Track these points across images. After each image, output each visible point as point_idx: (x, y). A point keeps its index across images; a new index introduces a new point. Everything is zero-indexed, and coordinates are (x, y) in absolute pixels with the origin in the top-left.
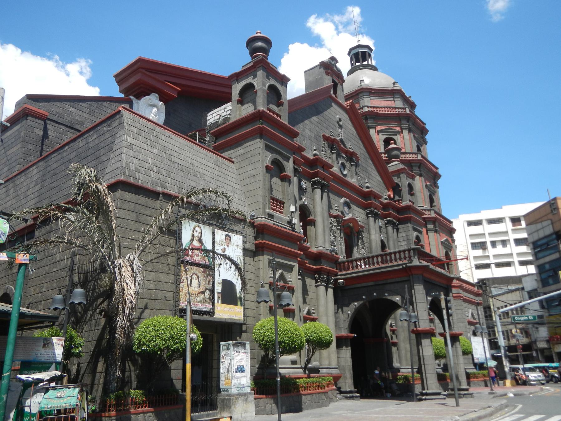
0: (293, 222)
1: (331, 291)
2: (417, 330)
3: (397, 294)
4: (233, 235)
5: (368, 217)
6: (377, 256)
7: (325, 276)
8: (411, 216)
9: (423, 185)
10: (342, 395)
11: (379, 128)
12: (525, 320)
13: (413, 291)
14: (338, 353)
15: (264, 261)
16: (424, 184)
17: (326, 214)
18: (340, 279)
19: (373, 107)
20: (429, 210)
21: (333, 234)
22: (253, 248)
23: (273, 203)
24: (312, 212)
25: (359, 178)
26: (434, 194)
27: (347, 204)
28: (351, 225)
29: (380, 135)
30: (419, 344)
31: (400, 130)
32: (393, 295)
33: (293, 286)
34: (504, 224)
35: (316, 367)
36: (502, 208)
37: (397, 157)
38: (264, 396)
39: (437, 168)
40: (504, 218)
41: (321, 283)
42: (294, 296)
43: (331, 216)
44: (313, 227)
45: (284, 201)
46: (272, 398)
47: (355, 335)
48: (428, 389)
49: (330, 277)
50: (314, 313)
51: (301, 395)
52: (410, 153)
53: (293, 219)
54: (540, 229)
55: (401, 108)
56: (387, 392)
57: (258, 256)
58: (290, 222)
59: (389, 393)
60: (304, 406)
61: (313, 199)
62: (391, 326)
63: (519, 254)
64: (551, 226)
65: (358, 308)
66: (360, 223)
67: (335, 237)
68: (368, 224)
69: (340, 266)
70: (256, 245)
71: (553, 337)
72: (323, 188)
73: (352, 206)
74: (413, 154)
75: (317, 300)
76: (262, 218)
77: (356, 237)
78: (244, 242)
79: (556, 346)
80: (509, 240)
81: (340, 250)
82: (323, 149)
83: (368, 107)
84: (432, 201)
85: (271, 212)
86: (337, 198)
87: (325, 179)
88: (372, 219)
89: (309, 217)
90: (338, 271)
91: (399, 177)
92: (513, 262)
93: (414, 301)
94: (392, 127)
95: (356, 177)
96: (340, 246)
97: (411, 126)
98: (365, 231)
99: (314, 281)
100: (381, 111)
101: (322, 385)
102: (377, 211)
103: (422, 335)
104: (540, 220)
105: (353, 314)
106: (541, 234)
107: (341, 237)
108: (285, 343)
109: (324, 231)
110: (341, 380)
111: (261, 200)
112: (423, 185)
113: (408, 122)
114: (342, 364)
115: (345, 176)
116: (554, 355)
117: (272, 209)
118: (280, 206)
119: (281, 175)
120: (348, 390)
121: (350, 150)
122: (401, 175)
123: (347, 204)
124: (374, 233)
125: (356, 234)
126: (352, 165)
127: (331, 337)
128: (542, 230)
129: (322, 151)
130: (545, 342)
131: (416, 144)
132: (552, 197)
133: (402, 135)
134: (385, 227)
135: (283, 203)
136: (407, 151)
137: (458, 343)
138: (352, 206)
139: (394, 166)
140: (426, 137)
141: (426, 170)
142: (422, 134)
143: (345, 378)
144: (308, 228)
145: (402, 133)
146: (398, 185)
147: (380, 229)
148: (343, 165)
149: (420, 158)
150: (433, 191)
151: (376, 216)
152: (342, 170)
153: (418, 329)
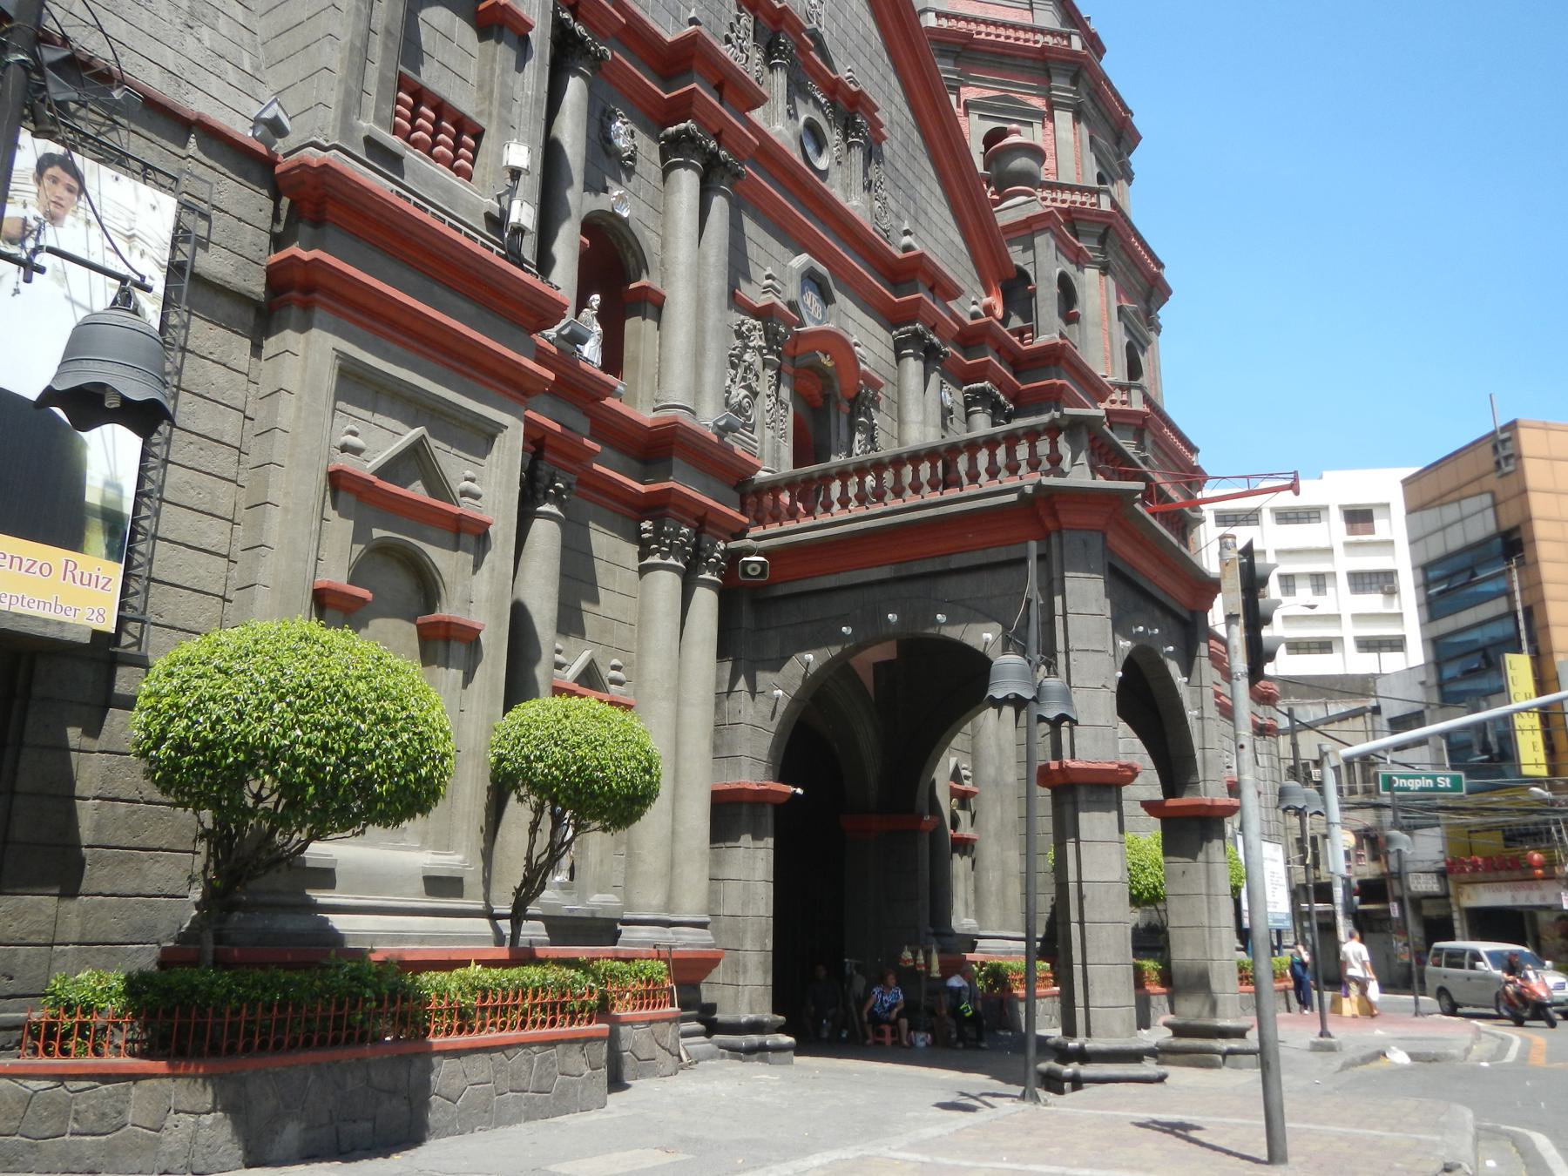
0: (513, 219)
1: (706, 601)
2: (1063, 770)
3: (988, 617)
4: (106, 172)
5: (899, 358)
6: (915, 458)
7: (685, 530)
8: (1063, 386)
9: (1108, 303)
10: (717, 1037)
11: (970, 93)
12: (1422, 789)
13: (1058, 600)
14: (716, 862)
15: (306, 358)
16: (1114, 305)
17: (716, 284)
18: (750, 552)
19: (957, 17)
20: (1122, 387)
21: (744, 379)
22: (256, 285)
23: (416, 114)
24: (653, 260)
25: (877, 204)
26: (1144, 349)
27: (811, 279)
28: (826, 361)
29: (974, 117)
30: (1065, 829)
31: (1045, 109)
32: (969, 621)
33: (485, 517)
34: (1324, 524)
35: (599, 915)
36: (1321, 478)
37: (1029, 179)
38: (161, 1066)
39: (1160, 265)
40: (1326, 508)
41: (665, 556)
42: (485, 567)
43: (735, 301)
44: (650, 324)
45: (482, 122)
46: (205, 1077)
47: (799, 791)
48: (1088, 1034)
49: (705, 537)
50: (619, 683)
51: (428, 1053)
52: (1072, 189)
53: (516, 204)
54: (1450, 525)
55: (1053, 33)
56: (913, 1027)
57: (280, 329)
58: (496, 222)
59: (927, 1030)
60: (436, 1115)
61: (662, 212)
62: (956, 776)
63: (1358, 618)
64: (1490, 513)
65: (816, 675)
66: (863, 366)
67: (756, 394)
68: (899, 384)
69: (760, 501)
70: (272, 273)
71: (1462, 862)
72: (711, 177)
73: (838, 295)
74: (1082, 190)
75: (640, 626)
76: (325, 149)
77: (844, 419)
78: (181, 235)
79: (1468, 889)
80: (1334, 574)
81: (767, 447)
82: (733, 36)
83: (939, 15)
84: (1134, 370)
85: (395, 142)
86: (775, 246)
87: (723, 136)
88: (913, 367)
89: (638, 278)
90: (746, 520)
91: (1029, 246)
92: (1341, 639)
93: (1060, 646)
94: (1017, 96)
95: (865, 195)
96: (769, 433)
97: (1084, 99)
98: (883, 404)
99: (633, 550)
100: (983, 33)
101: (576, 1004)
102: (936, 340)
103: (1082, 794)
104: (1456, 495)
105: (795, 700)
106: (1455, 540)
107: (782, 403)
108: (295, 761)
109: (698, 353)
110: (718, 974)
111: (335, 64)
112: (1108, 303)
113: (1074, 82)
114: (730, 906)
115: (824, 174)
116: (1456, 916)
117: (396, 130)
118: (458, 144)
119: (482, 6)
120: (745, 1017)
121: (852, 86)
122: (1037, 240)
123: (811, 279)
124: (920, 418)
125: (845, 406)
126: (850, 146)
127: (647, 771)
128: (1458, 527)
129: (728, 40)
130: (1435, 876)
131: (1096, 170)
132: (1502, 422)
133: (1049, 125)
134: (963, 416)
135: (478, 135)
136: (1062, 180)
137: (1217, 843)
138: (838, 295)
139: (1010, 212)
140: (1132, 158)
141: (1124, 257)
142: (1118, 144)
143: (738, 967)
144: (631, 325)
145: (1052, 120)
146: (1023, 276)
147: (944, 418)
148: (811, 127)
149: (1105, 205)
150: (1143, 336)
151: (931, 356)
152: (810, 149)
153: (1072, 764)
